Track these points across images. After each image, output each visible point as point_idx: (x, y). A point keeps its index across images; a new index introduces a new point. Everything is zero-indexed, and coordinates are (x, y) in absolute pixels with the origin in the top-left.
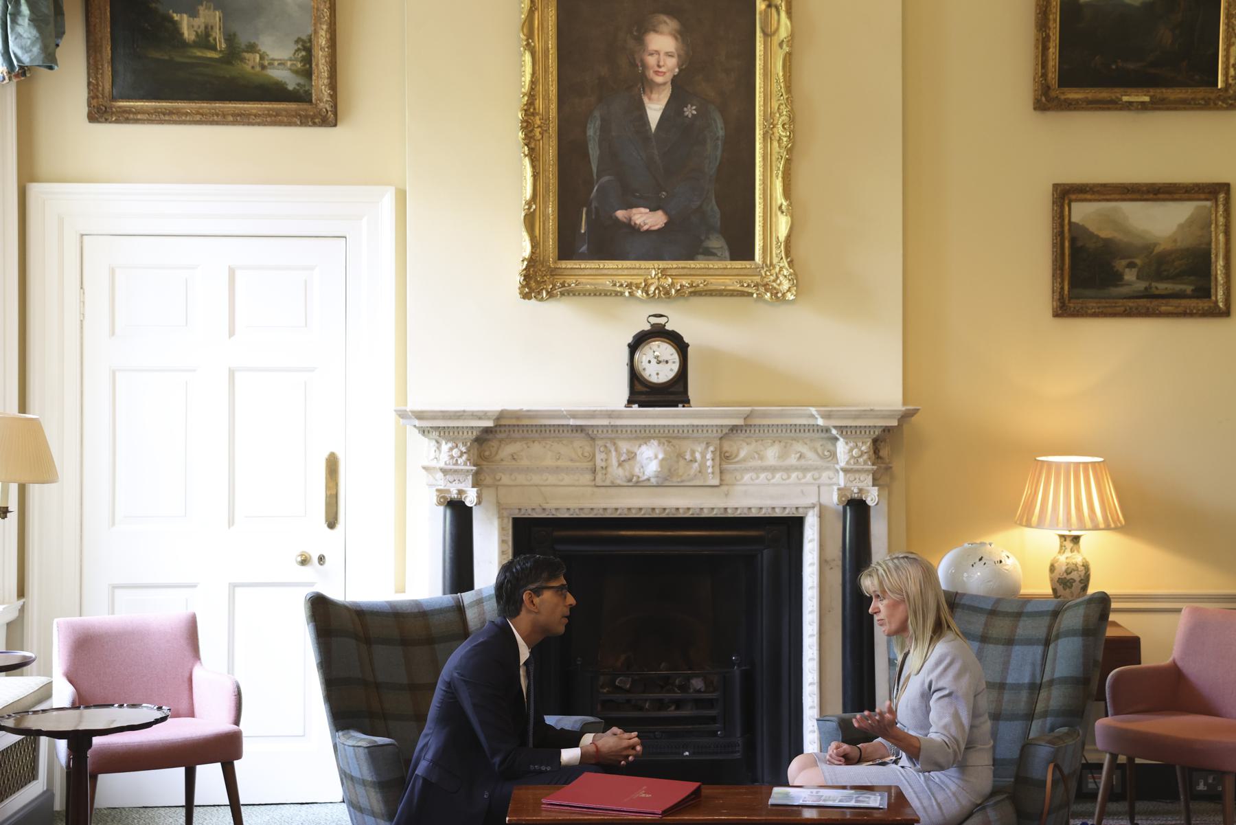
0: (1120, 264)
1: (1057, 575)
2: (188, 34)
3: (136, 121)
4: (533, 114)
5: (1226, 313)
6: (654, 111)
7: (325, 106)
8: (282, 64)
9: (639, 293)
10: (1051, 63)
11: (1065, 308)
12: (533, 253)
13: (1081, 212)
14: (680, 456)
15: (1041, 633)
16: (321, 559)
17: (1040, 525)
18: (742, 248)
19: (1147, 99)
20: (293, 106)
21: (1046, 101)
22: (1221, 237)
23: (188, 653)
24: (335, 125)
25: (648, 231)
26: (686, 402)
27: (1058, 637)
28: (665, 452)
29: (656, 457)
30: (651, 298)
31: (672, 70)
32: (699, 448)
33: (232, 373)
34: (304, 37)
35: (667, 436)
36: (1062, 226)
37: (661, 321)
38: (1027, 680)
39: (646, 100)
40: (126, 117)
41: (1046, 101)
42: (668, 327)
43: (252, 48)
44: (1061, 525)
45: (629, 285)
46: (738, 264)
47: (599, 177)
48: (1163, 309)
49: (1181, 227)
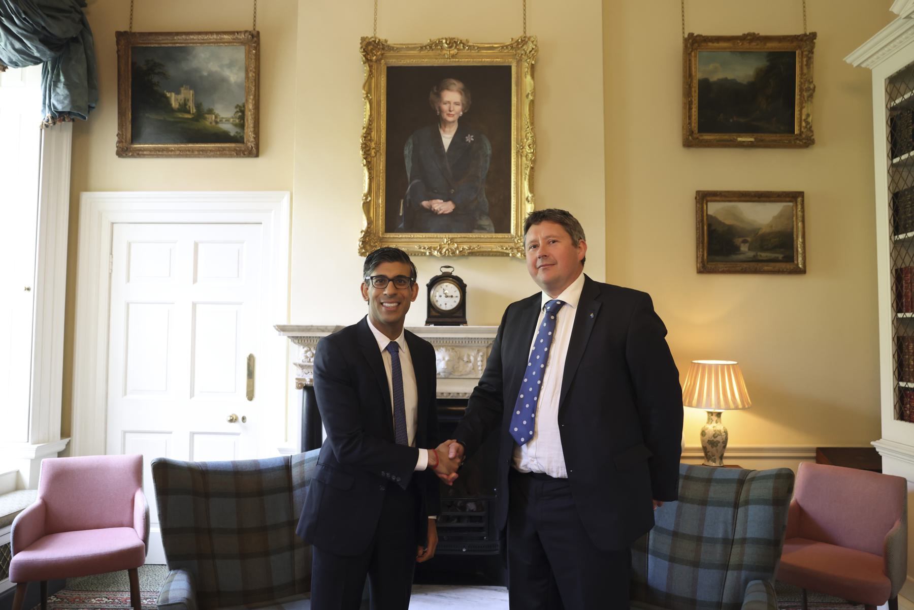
0: (738, 241)
1: (707, 438)
2: (174, 104)
3: (144, 156)
4: (370, 140)
5: (803, 272)
6: (447, 138)
7: (251, 144)
8: (228, 120)
9: (435, 253)
10: (693, 118)
11: (705, 268)
12: (368, 227)
13: (714, 208)
14: (460, 358)
15: (730, 496)
16: (244, 419)
17: (698, 405)
18: (502, 225)
19: (752, 139)
20: (233, 145)
21: (691, 141)
22: (800, 224)
23: (133, 482)
24: (257, 156)
25: (443, 215)
26: (465, 322)
27: (747, 503)
28: (450, 355)
29: (444, 359)
30: (444, 256)
31: (457, 113)
32: (473, 354)
33: (194, 305)
34: (240, 104)
35: (452, 345)
36: (703, 216)
37: (449, 270)
38: (720, 536)
39: (441, 132)
40: (138, 154)
41: (691, 141)
42: (454, 274)
43: (210, 112)
44: (713, 406)
45: (430, 248)
46: (500, 235)
48: (766, 268)
49: (775, 218)
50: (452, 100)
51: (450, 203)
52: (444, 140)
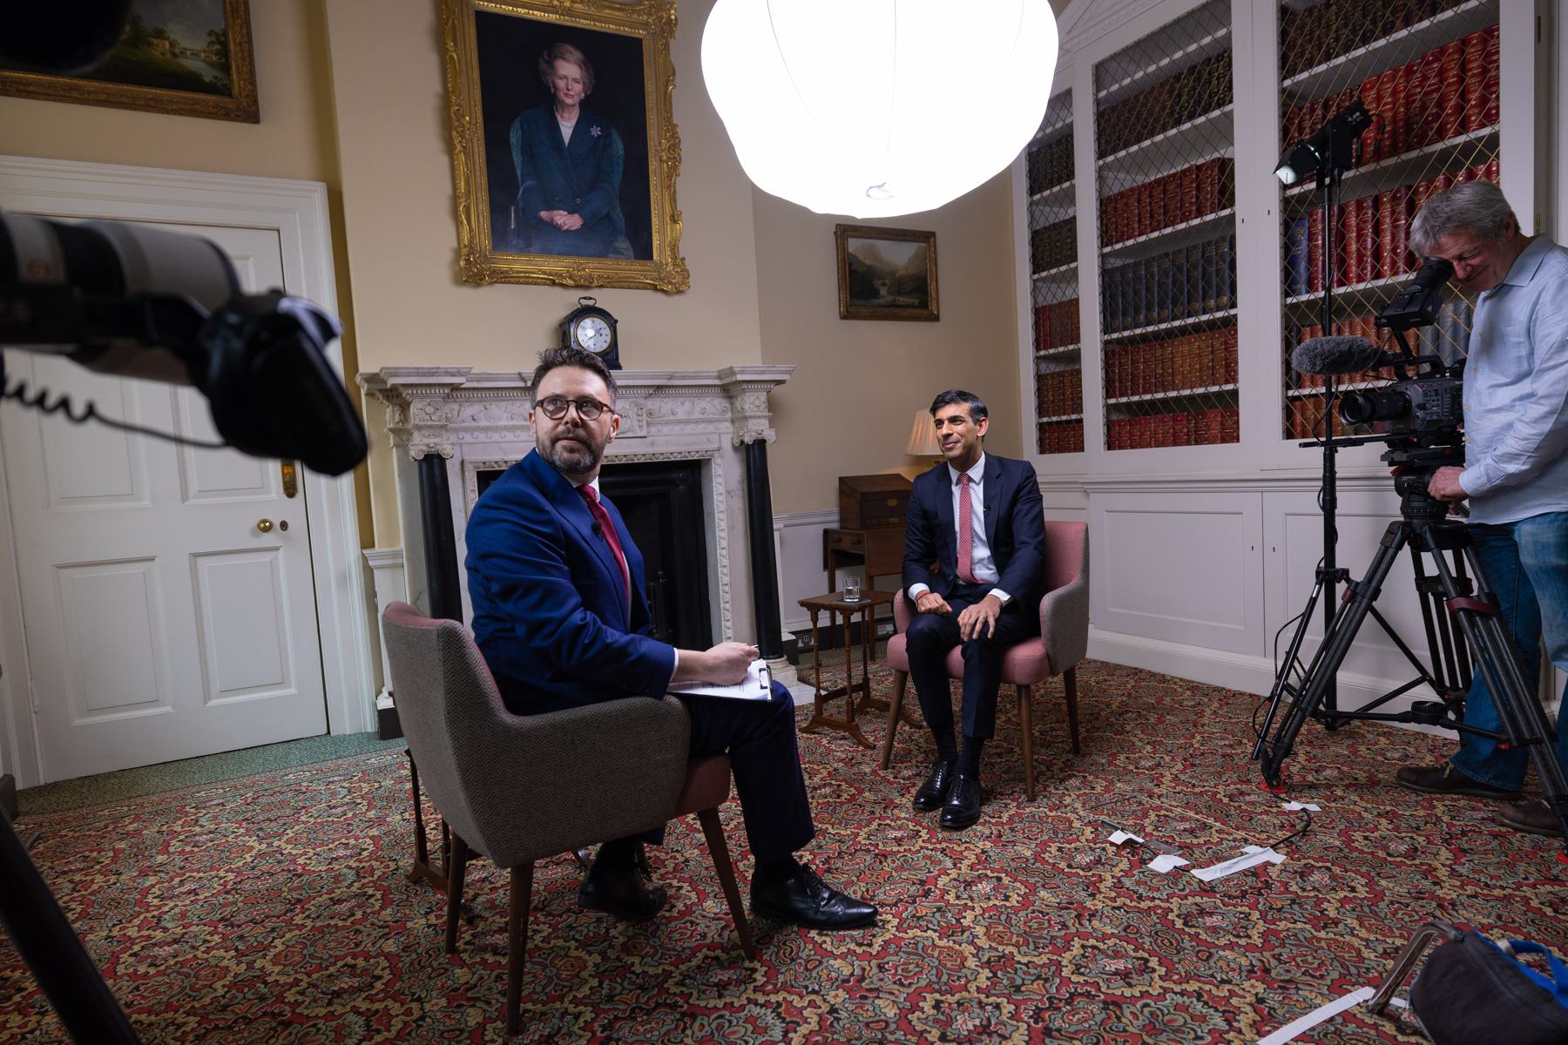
8: (195, 54)
34: (217, 30)
43: (160, 34)
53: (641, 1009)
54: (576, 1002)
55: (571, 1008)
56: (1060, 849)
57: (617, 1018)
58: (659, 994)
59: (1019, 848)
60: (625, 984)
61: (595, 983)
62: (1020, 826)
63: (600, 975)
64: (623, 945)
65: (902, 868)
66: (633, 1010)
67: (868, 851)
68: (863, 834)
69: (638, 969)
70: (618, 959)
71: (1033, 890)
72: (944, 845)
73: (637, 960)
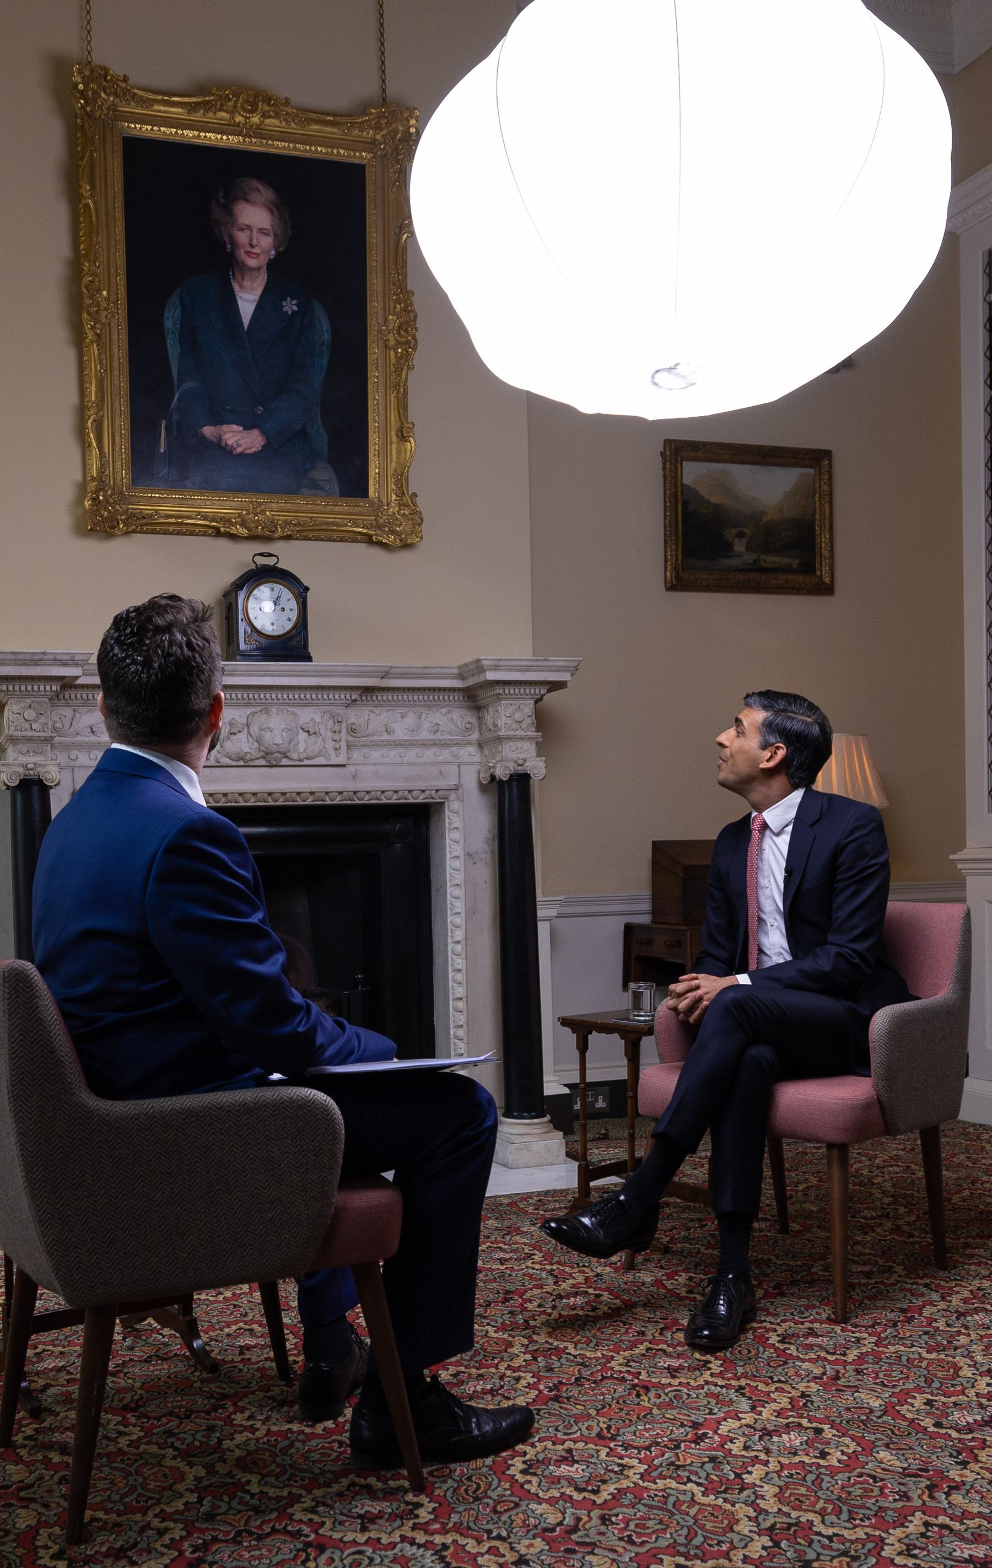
6: (247, 303)
25: (242, 455)
31: (268, 252)
37: (270, 561)
39: (236, 287)
47: (181, 382)
50: (255, 223)
51: (256, 432)
52: (240, 303)
53: (250, 1533)
54: (163, 1516)
55: (156, 1522)
56: (929, 1403)
57: (215, 1540)
58: (278, 1519)
59: (862, 1395)
60: (234, 1503)
61: (193, 1498)
62: (871, 1368)
63: (201, 1491)
64: (239, 1460)
65: (670, 1405)
66: (239, 1533)
67: (623, 1380)
68: (619, 1358)
69: (254, 1489)
70: (230, 1474)
71: (869, 1448)
72: (743, 1382)
73: (254, 1479)
